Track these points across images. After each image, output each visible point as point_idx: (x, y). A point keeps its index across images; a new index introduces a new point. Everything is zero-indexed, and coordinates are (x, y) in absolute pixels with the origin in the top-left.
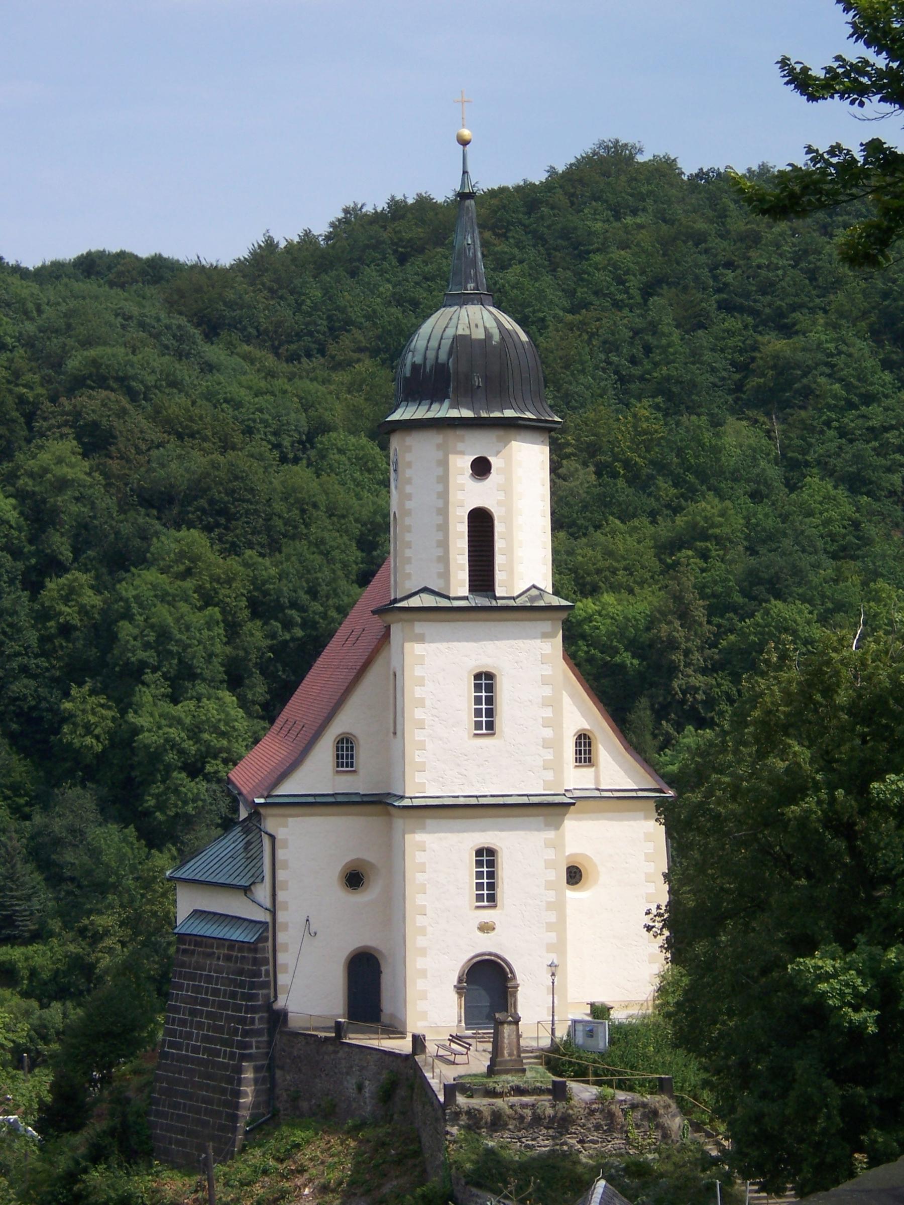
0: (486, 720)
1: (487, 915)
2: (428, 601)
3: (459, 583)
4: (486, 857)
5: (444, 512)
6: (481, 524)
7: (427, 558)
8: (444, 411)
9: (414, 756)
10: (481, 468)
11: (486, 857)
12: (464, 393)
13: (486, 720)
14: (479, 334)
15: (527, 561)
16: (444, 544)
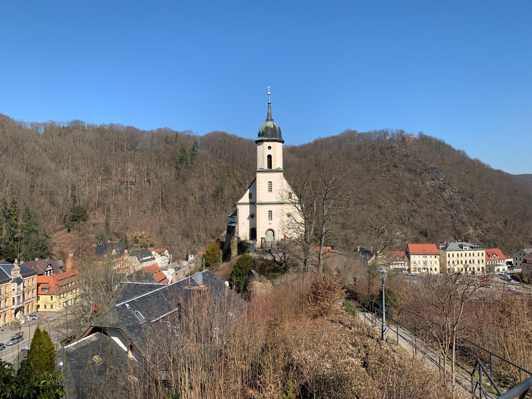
0: (270, 190)
1: (270, 222)
2: (261, 170)
3: (266, 167)
4: (270, 212)
5: (263, 155)
6: (270, 157)
7: (262, 163)
8: (263, 138)
9: (258, 195)
10: (270, 148)
11: (270, 212)
12: (267, 136)
13: (270, 190)
14: (269, 126)
15: (278, 163)
16: (263, 161)
